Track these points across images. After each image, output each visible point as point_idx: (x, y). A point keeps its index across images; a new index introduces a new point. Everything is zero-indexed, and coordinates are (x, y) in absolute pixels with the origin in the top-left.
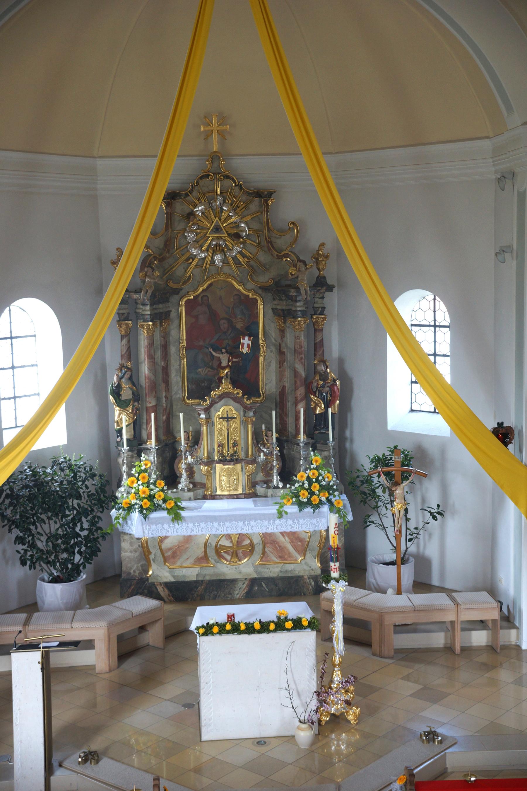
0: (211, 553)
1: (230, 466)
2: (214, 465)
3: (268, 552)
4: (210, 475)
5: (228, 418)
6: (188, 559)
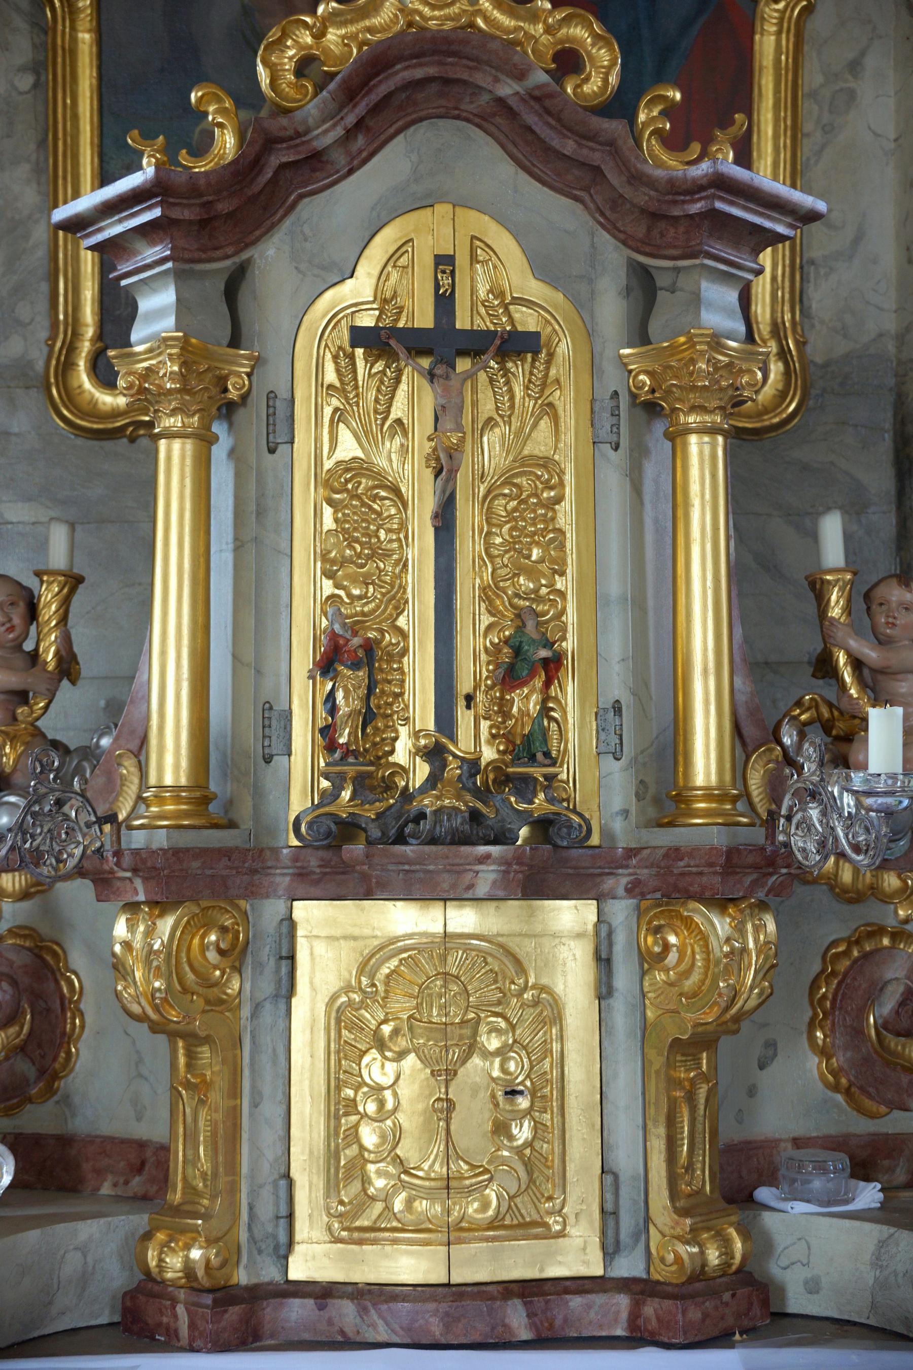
1: (464, 919)
2: (271, 910)
4: (218, 1025)
5: (437, 345)
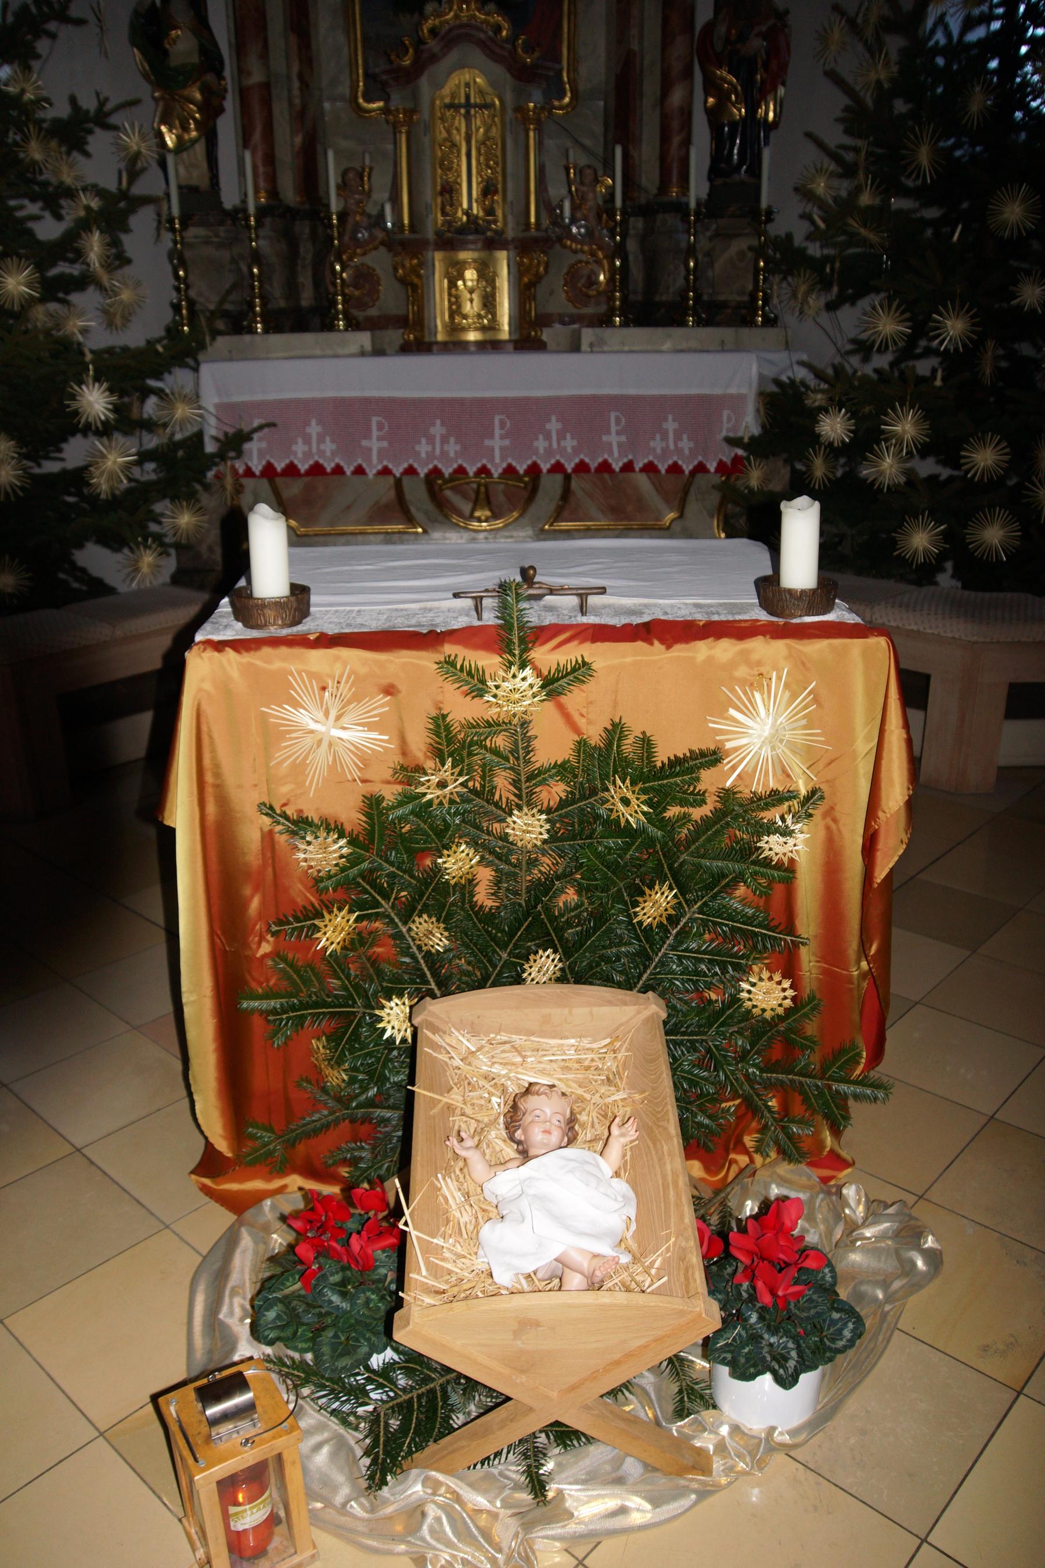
0: (416, 494)
3: (580, 494)
6: (349, 507)
